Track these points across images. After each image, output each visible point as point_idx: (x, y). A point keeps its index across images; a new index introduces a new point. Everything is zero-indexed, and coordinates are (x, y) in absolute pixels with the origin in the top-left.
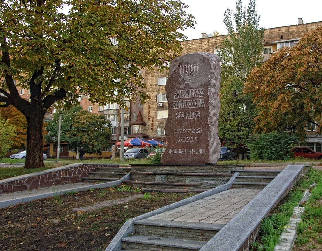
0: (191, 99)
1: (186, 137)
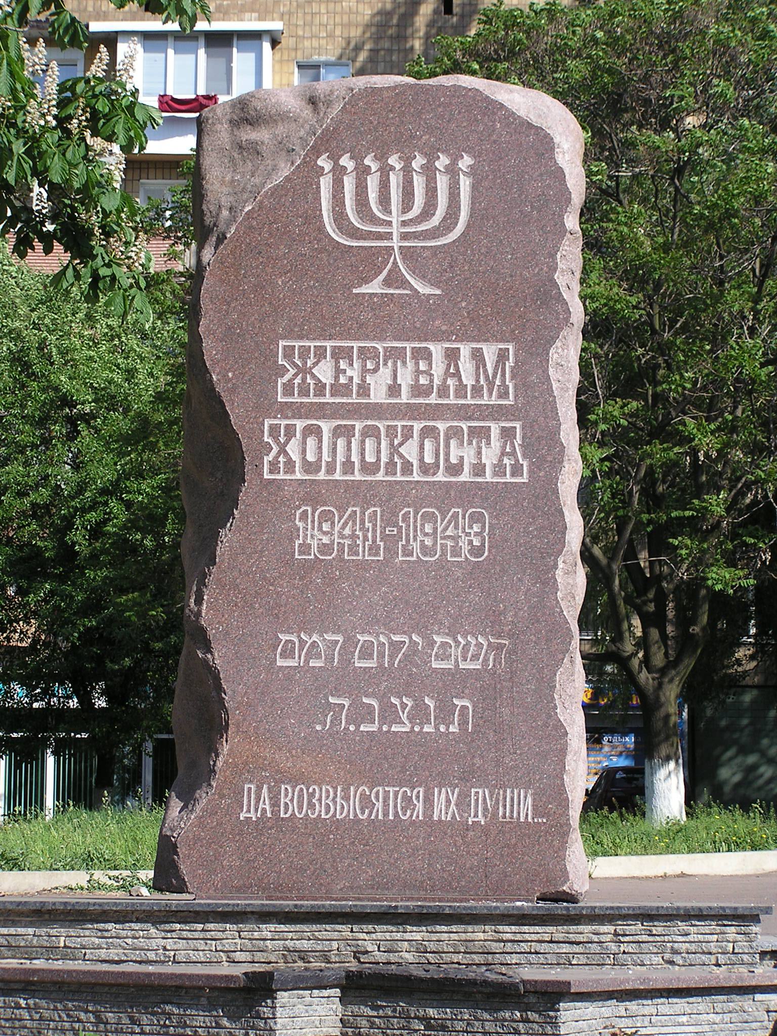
0: (412, 412)
1: (383, 699)
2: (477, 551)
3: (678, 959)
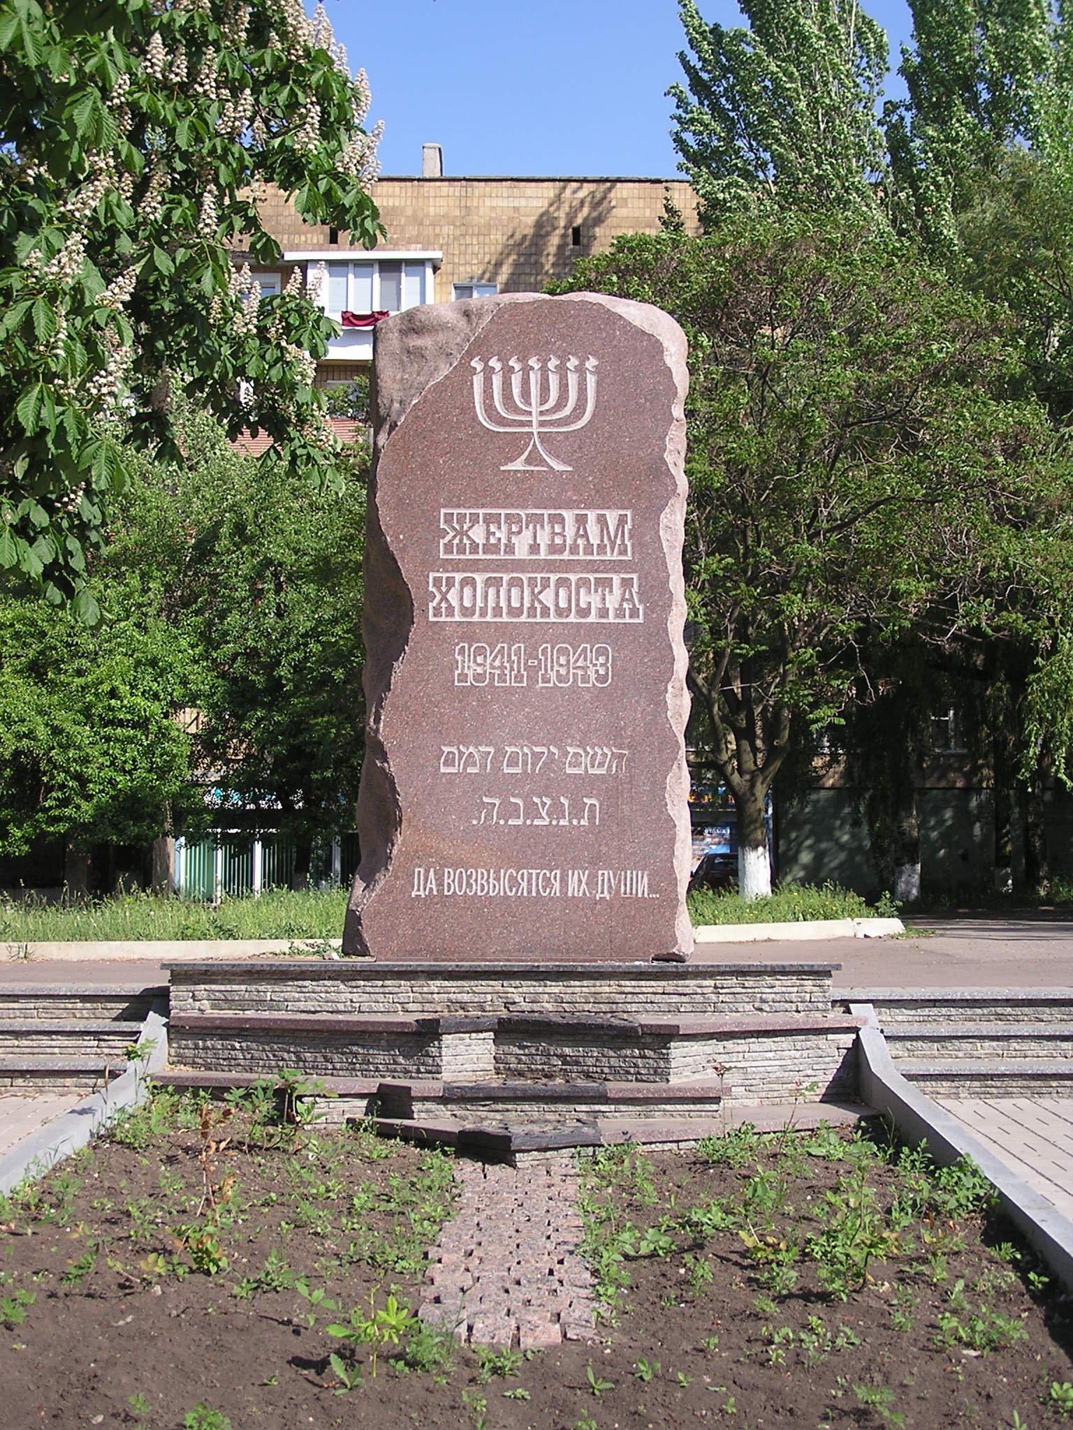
0: (550, 566)
2: (603, 679)
3: (765, 1007)
